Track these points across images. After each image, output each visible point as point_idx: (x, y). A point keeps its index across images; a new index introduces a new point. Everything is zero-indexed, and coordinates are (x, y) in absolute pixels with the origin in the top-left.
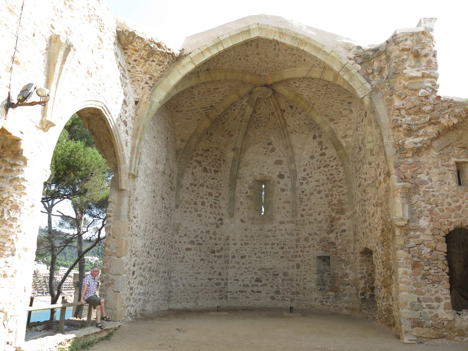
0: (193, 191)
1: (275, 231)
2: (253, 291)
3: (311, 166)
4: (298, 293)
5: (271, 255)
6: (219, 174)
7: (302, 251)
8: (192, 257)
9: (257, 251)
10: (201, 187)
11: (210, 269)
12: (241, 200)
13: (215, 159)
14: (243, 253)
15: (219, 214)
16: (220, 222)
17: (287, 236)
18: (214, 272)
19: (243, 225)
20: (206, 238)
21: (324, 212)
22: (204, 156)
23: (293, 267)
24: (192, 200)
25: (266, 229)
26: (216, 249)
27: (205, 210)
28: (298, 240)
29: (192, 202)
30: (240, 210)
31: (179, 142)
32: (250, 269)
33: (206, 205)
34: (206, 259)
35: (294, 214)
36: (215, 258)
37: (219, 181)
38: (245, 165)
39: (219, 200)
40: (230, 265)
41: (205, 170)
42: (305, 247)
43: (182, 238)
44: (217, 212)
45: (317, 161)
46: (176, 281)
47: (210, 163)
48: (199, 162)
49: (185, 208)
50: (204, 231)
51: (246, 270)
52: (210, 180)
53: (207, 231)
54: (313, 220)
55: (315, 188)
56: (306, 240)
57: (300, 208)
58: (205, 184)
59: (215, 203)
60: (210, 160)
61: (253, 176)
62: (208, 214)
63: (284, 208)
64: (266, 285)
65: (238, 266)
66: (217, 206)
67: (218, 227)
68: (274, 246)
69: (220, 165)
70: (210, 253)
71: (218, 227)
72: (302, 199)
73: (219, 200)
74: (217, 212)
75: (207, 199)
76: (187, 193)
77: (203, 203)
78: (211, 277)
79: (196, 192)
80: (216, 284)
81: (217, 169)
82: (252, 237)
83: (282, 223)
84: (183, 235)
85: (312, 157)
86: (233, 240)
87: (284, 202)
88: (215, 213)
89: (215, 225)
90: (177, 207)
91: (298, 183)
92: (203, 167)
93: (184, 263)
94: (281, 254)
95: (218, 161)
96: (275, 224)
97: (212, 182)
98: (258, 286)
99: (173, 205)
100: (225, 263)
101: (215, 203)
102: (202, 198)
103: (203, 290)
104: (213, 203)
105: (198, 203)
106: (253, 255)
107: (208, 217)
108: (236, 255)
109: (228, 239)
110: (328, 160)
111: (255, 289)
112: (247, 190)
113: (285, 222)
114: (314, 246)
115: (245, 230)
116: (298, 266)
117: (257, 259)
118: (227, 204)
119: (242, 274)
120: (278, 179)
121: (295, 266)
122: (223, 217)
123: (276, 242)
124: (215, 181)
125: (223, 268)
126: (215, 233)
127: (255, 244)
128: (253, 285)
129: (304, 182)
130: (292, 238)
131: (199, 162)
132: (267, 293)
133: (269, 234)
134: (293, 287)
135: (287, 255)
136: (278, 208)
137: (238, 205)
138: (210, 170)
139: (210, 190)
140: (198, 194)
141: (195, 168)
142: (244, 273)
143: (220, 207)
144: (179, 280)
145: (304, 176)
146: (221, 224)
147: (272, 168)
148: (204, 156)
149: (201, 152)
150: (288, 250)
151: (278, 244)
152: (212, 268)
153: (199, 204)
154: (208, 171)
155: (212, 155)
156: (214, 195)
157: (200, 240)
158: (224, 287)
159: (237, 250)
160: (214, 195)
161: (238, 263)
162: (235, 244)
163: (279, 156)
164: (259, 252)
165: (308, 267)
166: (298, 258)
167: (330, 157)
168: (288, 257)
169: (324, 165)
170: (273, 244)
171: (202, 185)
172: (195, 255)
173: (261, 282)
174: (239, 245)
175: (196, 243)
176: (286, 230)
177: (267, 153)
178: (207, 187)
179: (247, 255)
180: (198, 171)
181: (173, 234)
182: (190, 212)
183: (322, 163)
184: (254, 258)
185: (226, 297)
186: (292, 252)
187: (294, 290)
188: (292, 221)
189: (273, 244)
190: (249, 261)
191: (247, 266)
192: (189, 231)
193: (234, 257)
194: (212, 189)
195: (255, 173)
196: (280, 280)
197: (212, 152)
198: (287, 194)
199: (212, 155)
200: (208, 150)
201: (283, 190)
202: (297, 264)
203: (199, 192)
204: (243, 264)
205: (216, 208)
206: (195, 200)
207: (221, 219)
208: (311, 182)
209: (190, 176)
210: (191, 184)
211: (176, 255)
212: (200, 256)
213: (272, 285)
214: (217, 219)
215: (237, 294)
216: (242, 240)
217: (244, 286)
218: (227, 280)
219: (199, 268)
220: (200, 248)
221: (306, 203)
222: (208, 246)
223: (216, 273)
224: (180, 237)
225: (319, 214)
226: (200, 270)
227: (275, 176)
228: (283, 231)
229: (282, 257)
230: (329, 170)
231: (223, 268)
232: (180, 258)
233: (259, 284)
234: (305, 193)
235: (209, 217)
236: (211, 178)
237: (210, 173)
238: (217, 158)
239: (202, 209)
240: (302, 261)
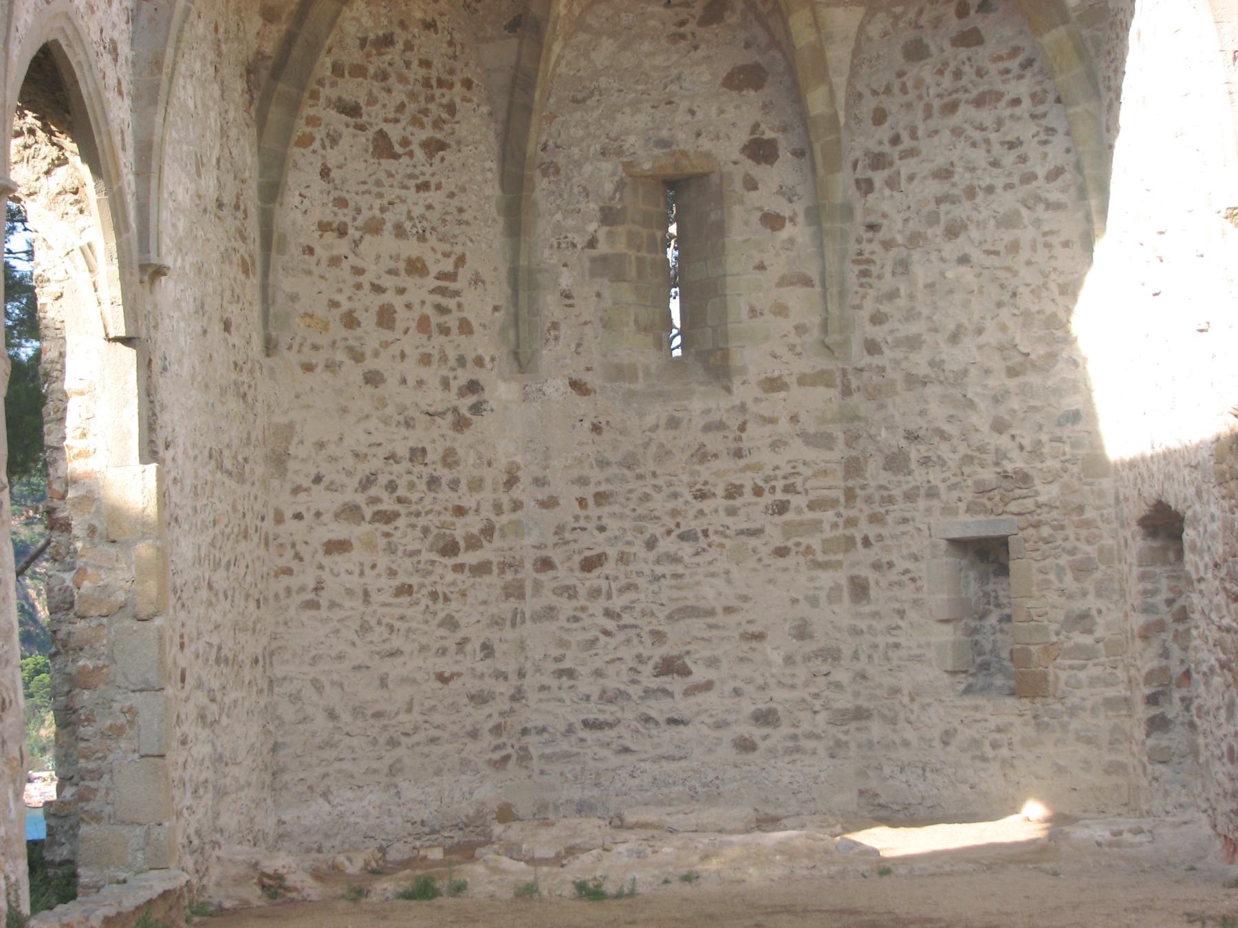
0: (335, 261)
1: (742, 428)
2: (648, 719)
3: (912, 96)
4: (860, 714)
5: (727, 542)
6: (449, 155)
7: (875, 519)
8: (354, 581)
9: (653, 529)
10: (368, 237)
11: (442, 632)
12: (566, 280)
13: (427, 83)
14: (594, 542)
15: (461, 361)
16: (472, 399)
17: (798, 450)
18: (462, 644)
19: (583, 405)
20: (411, 486)
21: (980, 331)
22: (372, 70)
23: (834, 595)
24: (334, 304)
25: (700, 422)
26: (459, 534)
27: (395, 349)
28: (853, 468)
29: (337, 313)
30: (564, 331)
32: (627, 619)
33: (400, 325)
34: (422, 585)
35: (833, 338)
36: (460, 577)
37: (452, 195)
38: (575, 101)
39: (456, 293)
40: (531, 605)
42: (890, 500)
43: (302, 496)
44: (452, 355)
45: (941, 72)
46: (295, 698)
47: (401, 107)
48: (352, 110)
49: (306, 349)
50: (402, 450)
51: (610, 625)
52: (411, 194)
53: (413, 451)
54: (923, 370)
55: (932, 206)
56: (896, 462)
57: (859, 307)
58: (388, 216)
59: (442, 310)
60: (399, 95)
61: (620, 152)
62: (413, 370)
63: (781, 310)
64: (708, 686)
65: (566, 607)
66: (452, 321)
67: (461, 424)
68: (738, 502)
69: (451, 109)
70: (434, 556)
72: (869, 261)
73: (456, 293)
74: (452, 355)
75: (401, 291)
76: (309, 273)
77: (386, 317)
78: (446, 665)
79: (345, 265)
80: (472, 698)
81: (439, 136)
82: (630, 462)
83: (773, 384)
84: (306, 483)
85: (916, 51)
86: (539, 482)
87: (784, 282)
88: (444, 359)
89: (450, 417)
90: (270, 347)
91: (842, 185)
92: (371, 133)
93: (324, 613)
94: (776, 538)
95: (437, 92)
96: (744, 392)
97: (417, 202)
98: (669, 694)
100: (508, 596)
101: (442, 310)
102: (378, 289)
103: (416, 729)
104: (429, 310)
105: (361, 315)
106: (638, 548)
107: (411, 382)
108: (556, 556)
109: (511, 482)
110: (993, 68)
111: (658, 708)
112: (592, 227)
113: (791, 381)
114: (932, 494)
115: (596, 428)
116: (860, 589)
117: (659, 570)
118: (496, 309)
119: (594, 641)
120: (748, 165)
121: (846, 593)
122: (481, 375)
123: (748, 480)
124: (433, 196)
125: (497, 622)
126: (449, 458)
127: (646, 498)
128: (648, 693)
129: (879, 178)
130: (827, 455)
131: (352, 110)
132: (719, 726)
133: (713, 442)
134: (838, 686)
135: (805, 541)
136: (753, 312)
137: (550, 305)
138: (405, 142)
139: (411, 248)
140: (358, 271)
141: (334, 140)
142: (603, 639)
143: (465, 327)
144: (309, 693)
145: (877, 149)
146: (476, 409)
147: (714, 110)
148: (372, 70)
149: (354, 56)
150: (810, 515)
151: (758, 492)
152: (451, 623)
153: (368, 320)
154: (398, 149)
155: (408, 64)
156: (434, 270)
157: (385, 495)
158: (512, 711)
159: (559, 530)
160: (434, 270)
161: (569, 592)
162: (550, 503)
163: (748, 45)
164: (669, 532)
165: (907, 593)
166: (861, 552)
167: (1004, 52)
168: (809, 550)
169: (975, 92)
170: (733, 492)
171: (374, 227)
172: (367, 570)
173: (685, 672)
174: (567, 511)
175: (368, 512)
176: (794, 419)
177: (687, 29)
178: (400, 232)
179: (612, 553)
182: (331, 366)
183: (964, 81)
184: (644, 561)
185: (524, 756)
186: (826, 526)
187: (843, 702)
188: (823, 372)
189: (733, 492)
190: (623, 581)
191: (617, 603)
192: (333, 459)
193: (546, 564)
194: (422, 238)
195: (632, 139)
196: (777, 657)
197: (408, 46)
198: (791, 241)
199: (408, 64)
200: (388, 41)
201: (773, 221)
202: (853, 580)
203: (359, 263)
204: (595, 593)
205: (445, 331)
206: (346, 306)
207: (473, 387)
208: (911, 178)
209: (318, 184)
210: (324, 227)
211: (285, 580)
212: (392, 573)
213: (739, 684)
214: (455, 385)
215: (573, 739)
216: (583, 481)
217: (607, 697)
218: (521, 674)
219: (391, 628)
220: (387, 535)
221: (888, 283)
222: (422, 522)
223: (468, 647)
224: (296, 490)
225: (954, 338)
226: (397, 642)
227: (728, 152)
228: (784, 426)
229: (781, 552)
230: (999, 123)
231: (497, 622)
232: (302, 589)
233: (675, 684)
234: (883, 235)
235: (420, 383)
236: (412, 183)
237: (405, 160)
238: (434, 74)
239: (385, 345)
240: (877, 566)
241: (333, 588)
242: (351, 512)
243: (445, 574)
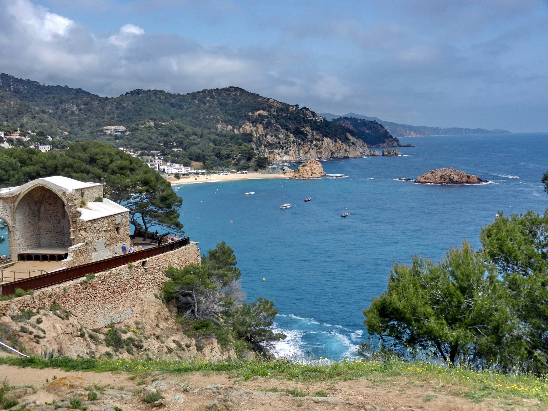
41: (50, 204)
77: (51, 217)
99: (37, 221)
180: (47, 205)
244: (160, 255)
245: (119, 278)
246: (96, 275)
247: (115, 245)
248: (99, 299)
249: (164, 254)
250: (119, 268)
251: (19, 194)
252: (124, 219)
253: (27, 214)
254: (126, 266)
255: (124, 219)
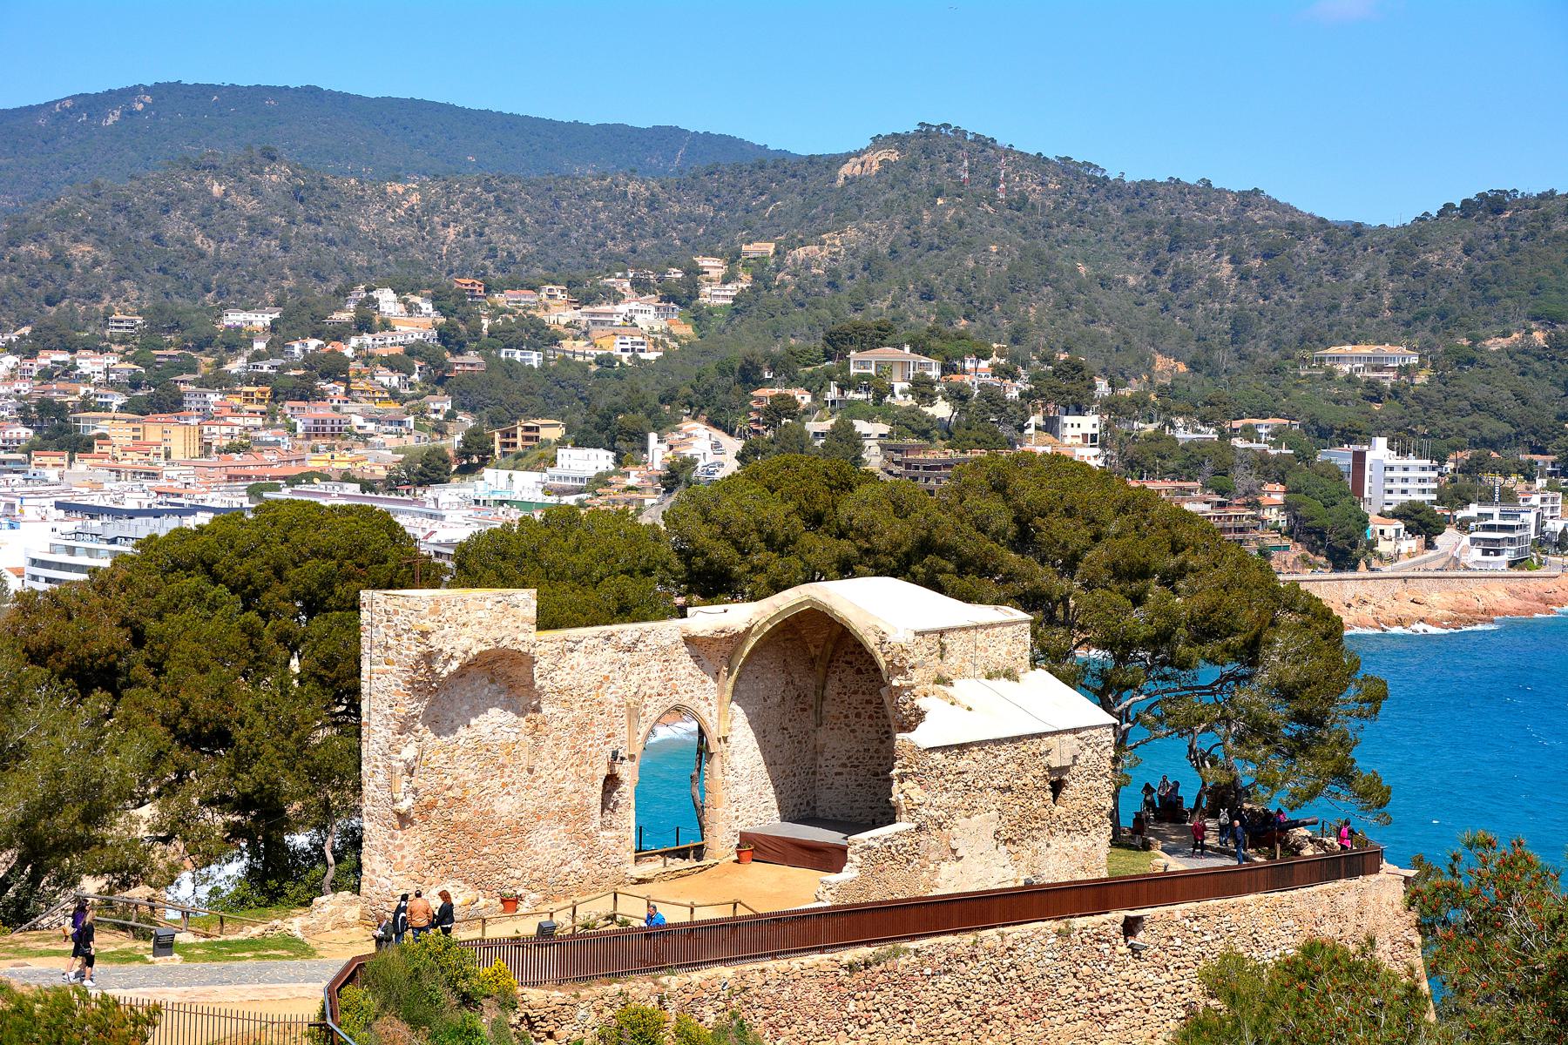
31: (812, 649)
41: (859, 671)
62: (866, 728)
67: (882, 742)
71: (882, 742)
77: (858, 715)
99: (811, 726)
139: (867, 697)
171: (855, 693)
181: (814, 759)
241: (837, 784)
242: (844, 765)
243: (874, 781)
244: (1211, 903)
245: (1013, 966)
246: (913, 945)
247: (1041, 844)
248: (915, 1032)
249: (1232, 901)
250: (1015, 932)
251: (749, 630)
252: (1089, 751)
253: (777, 699)
254: (1051, 925)
255: (1089, 751)
